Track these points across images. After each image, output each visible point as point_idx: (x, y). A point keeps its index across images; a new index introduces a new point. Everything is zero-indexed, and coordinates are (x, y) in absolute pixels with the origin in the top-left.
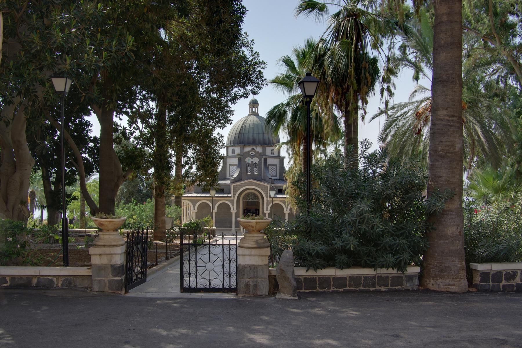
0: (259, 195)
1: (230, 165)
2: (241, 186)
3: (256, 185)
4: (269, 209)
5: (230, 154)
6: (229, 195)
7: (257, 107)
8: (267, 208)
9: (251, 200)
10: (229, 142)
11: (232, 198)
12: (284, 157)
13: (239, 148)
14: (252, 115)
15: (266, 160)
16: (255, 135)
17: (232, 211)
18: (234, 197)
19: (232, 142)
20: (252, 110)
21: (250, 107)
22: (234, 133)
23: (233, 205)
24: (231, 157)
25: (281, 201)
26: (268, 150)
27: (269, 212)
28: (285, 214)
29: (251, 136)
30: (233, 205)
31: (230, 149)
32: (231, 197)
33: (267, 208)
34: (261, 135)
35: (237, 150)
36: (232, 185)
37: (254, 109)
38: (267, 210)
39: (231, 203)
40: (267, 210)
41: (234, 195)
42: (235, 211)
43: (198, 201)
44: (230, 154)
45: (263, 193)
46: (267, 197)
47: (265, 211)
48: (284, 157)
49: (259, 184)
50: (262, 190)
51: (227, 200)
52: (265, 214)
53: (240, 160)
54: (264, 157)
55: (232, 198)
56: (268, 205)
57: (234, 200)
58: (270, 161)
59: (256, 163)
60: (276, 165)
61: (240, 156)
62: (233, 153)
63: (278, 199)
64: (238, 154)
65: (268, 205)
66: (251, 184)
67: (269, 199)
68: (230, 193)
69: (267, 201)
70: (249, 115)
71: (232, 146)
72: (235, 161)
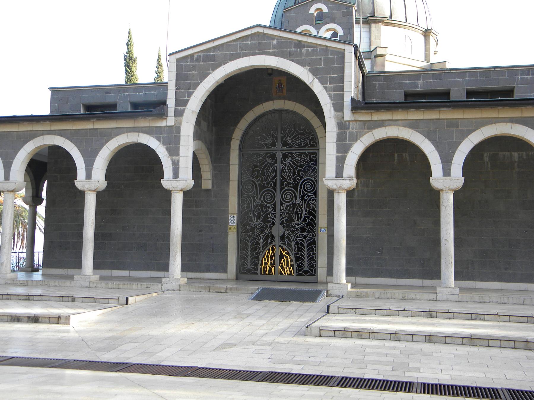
8: (341, 161)
11: (170, 121)
17: (167, 182)
18: (179, 114)
25: (414, 125)
30: (174, 150)
33: (341, 161)
38: (339, 174)
40: (339, 174)
45: (317, 88)
46: (338, 107)
49: (299, 44)
50: (314, 72)
51: (149, 131)
55: (170, 121)
56: (343, 149)
63: (399, 115)
65: (343, 149)
67: (348, 115)
69: (342, 125)
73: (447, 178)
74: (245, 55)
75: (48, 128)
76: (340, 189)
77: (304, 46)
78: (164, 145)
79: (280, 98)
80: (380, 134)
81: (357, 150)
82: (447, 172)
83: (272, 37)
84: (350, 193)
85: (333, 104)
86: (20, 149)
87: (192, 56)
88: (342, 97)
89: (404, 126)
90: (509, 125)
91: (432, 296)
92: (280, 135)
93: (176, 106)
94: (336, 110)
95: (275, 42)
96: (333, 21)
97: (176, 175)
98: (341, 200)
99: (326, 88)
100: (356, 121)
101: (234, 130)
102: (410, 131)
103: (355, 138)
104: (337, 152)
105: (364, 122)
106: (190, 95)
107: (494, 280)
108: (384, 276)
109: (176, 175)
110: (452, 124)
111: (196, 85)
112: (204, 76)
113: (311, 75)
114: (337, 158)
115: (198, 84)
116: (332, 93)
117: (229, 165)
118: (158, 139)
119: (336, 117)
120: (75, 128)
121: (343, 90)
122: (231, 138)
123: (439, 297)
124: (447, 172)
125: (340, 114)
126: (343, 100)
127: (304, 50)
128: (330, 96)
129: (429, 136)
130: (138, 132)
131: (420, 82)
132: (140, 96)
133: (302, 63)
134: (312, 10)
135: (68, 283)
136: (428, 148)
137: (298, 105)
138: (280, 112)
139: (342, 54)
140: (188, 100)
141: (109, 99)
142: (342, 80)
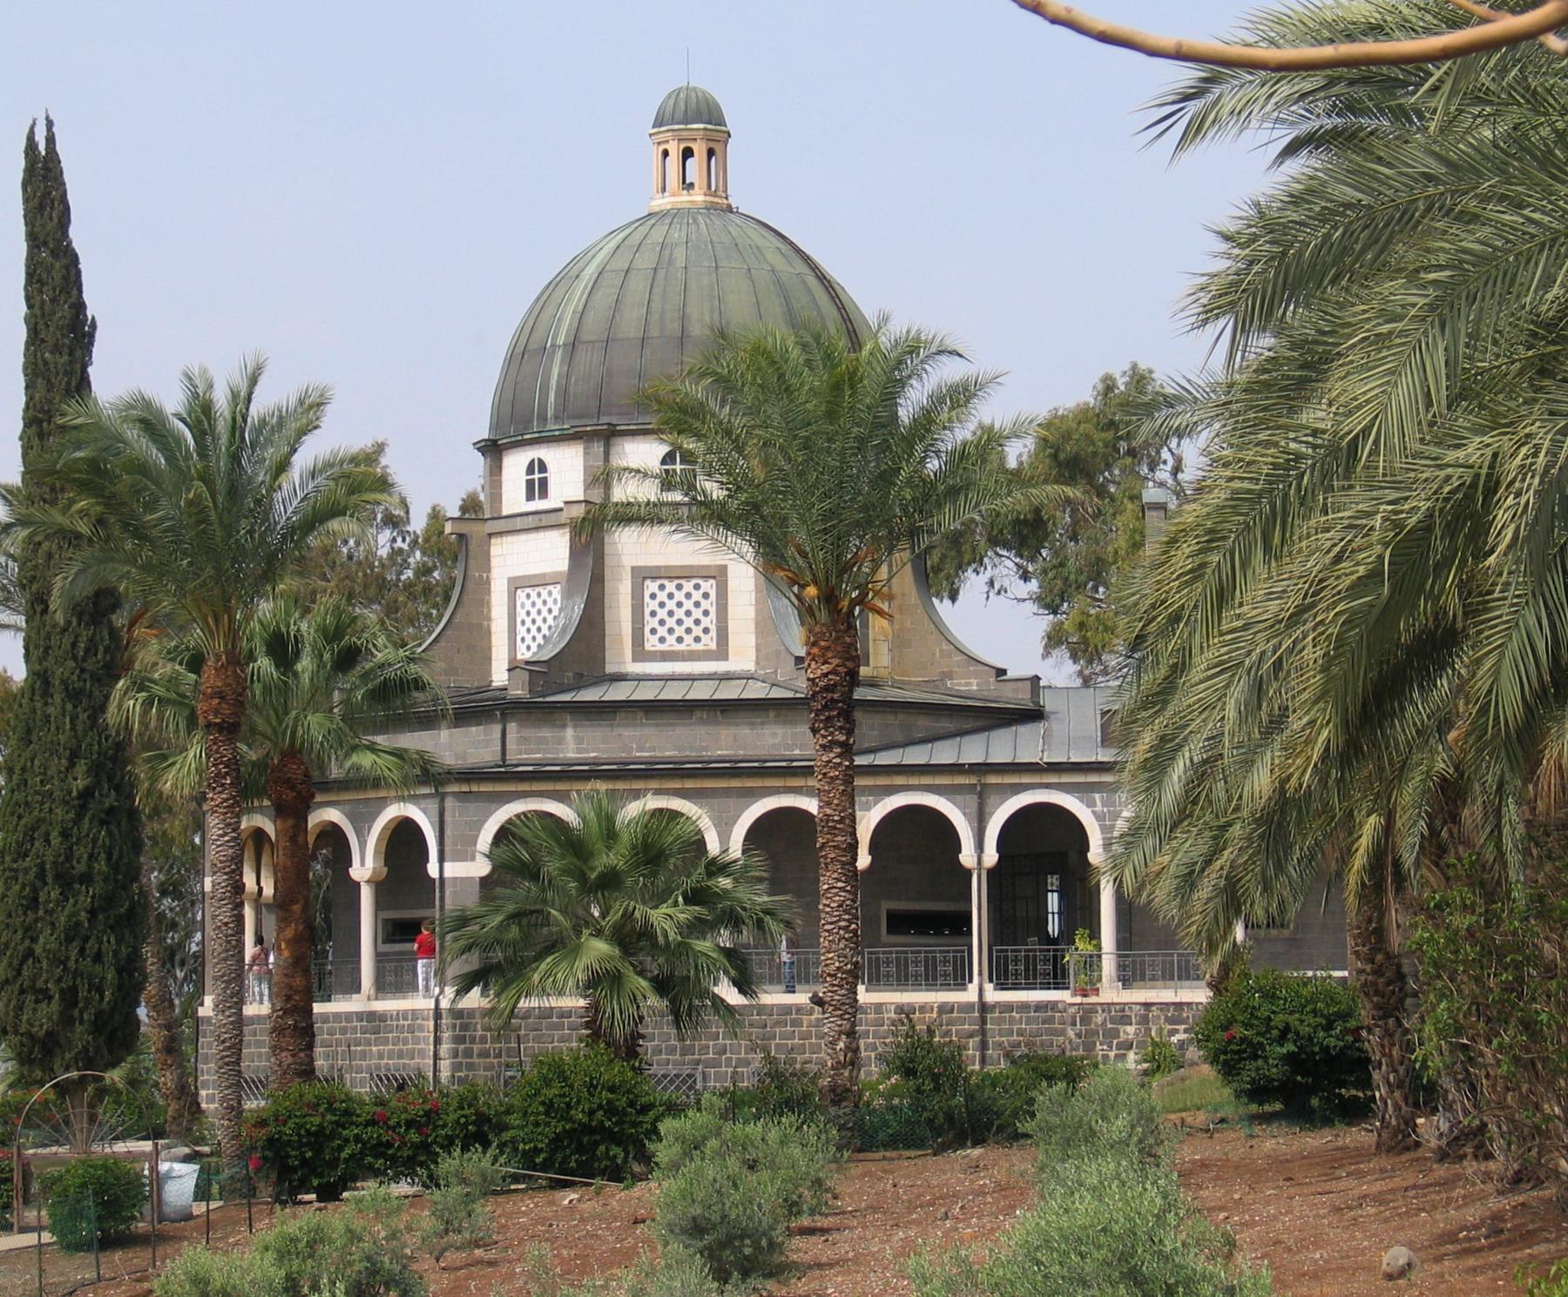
5: (514, 498)
62: (537, 487)
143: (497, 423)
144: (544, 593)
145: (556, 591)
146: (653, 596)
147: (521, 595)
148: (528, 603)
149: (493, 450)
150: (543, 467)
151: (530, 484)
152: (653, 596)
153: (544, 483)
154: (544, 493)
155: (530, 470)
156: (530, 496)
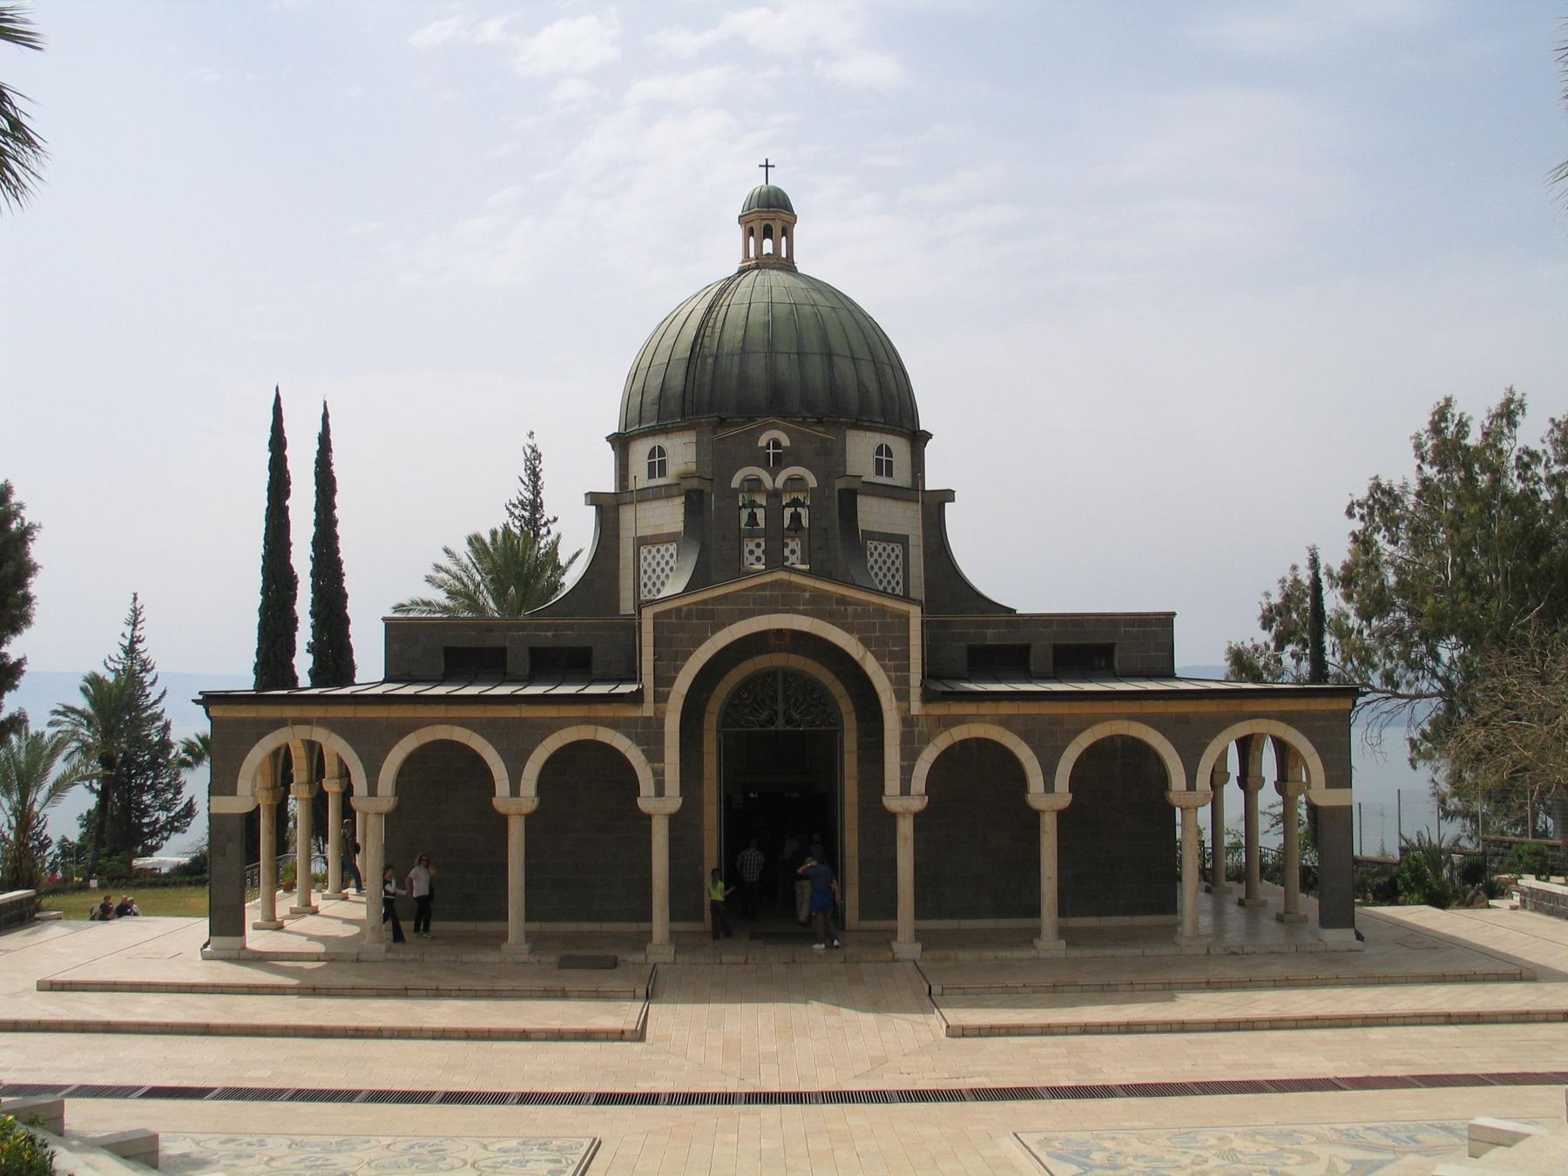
0: (837, 689)
1: (641, 542)
2: (711, 618)
3: (820, 607)
4: (919, 782)
5: (640, 476)
6: (633, 688)
7: (787, 232)
9: (780, 725)
10: (634, 413)
11: (648, 709)
12: (948, 495)
13: (690, 437)
14: (757, 267)
15: (848, 500)
16: (783, 363)
17: (646, 802)
18: (661, 698)
19: (651, 411)
20: (759, 247)
21: (751, 232)
22: (662, 358)
23: (655, 754)
24: (646, 495)
25: (1006, 722)
26: (861, 450)
27: (918, 803)
28: (1036, 815)
29: (757, 367)
30: (655, 754)
31: (640, 452)
32: (637, 698)
34: (815, 365)
35: (681, 452)
36: (648, 614)
37: (768, 246)
38: (905, 790)
39: (637, 739)
40: (905, 790)
41: (664, 681)
42: (673, 801)
43: (403, 729)
44: (640, 476)
45: (871, 666)
46: (902, 695)
47: (893, 800)
48: (948, 495)
49: (843, 601)
50: (866, 643)
52: (892, 817)
53: (695, 504)
54: (839, 484)
55: (648, 709)
56: (910, 755)
57: (658, 722)
58: (873, 514)
59: (795, 503)
60: (903, 540)
61: (693, 484)
62: (657, 466)
63: (987, 708)
64: (684, 477)
65: (910, 755)
66: (785, 599)
67: (916, 707)
68: (632, 675)
69: (907, 721)
70: (741, 272)
71: (652, 432)
72: (669, 516)
73: (1049, 794)
74: (761, 613)
75: (443, 715)
76: (907, 811)
77: (850, 604)
78: (638, 744)
79: (781, 650)
80: (960, 733)
81: (929, 756)
82: (1049, 787)
83: (803, 588)
84: (917, 816)
85: (895, 691)
86: (392, 746)
87: (678, 610)
88: (907, 681)
89: (993, 723)
90: (1126, 723)
91: (1032, 953)
92: (780, 707)
93: (655, 685)
94: (898, 699)
95: (807, 595)
96: (798, 463)
97: (660, 791)
98: (905, 828)
99: (884, 667)
100: (927, 715)
101: (708, 699)
102: (1001, 729)
103: (927, 740)
104: (902, 759)
105: (939, 717)
106: (677, 669)
107: (1091, 914)
108: (941, 918)
109: (660, 791)
110: (1056, 720)
111: (687, 656)
112: (699, 642)
113: (861, 647)
114: (902, 768)
115: (689, 654)
116: (893, 674)
117: (701, 754)
118: (629, 736)
119: (898, 708)
120: (488, 715)
121: (908, 670)
122: (703, 713)
123: (1042, 954)
124: (1049, 787)
125: (905, 704)
126: (908, 684)
127: (850, 609)
128: (889, 677)
129: (1025, 736)
130: (595, 723)
131: (990, 632)
132: (547, 638)
133: (848, 629)
134: (762, 442)
135: (490, 957)
136: (1025, 754)
137: (809, 661)
138: (789, 675)
139: (905, 619)
140: (675, 679)
141: (493, 641)
142: (906, 656)
143: (626, 421)
144: (663, 549)
145: (673, 548)
146: (751, 552)
147: (644, 551)
148: (649, 558)
149: (621, 442)
150: (662, 452)
151: (651, 466)
152: (751, 552)
153: (663, 464)
154: (663, 473)
155: (652, 455)
156: (651, 475)
